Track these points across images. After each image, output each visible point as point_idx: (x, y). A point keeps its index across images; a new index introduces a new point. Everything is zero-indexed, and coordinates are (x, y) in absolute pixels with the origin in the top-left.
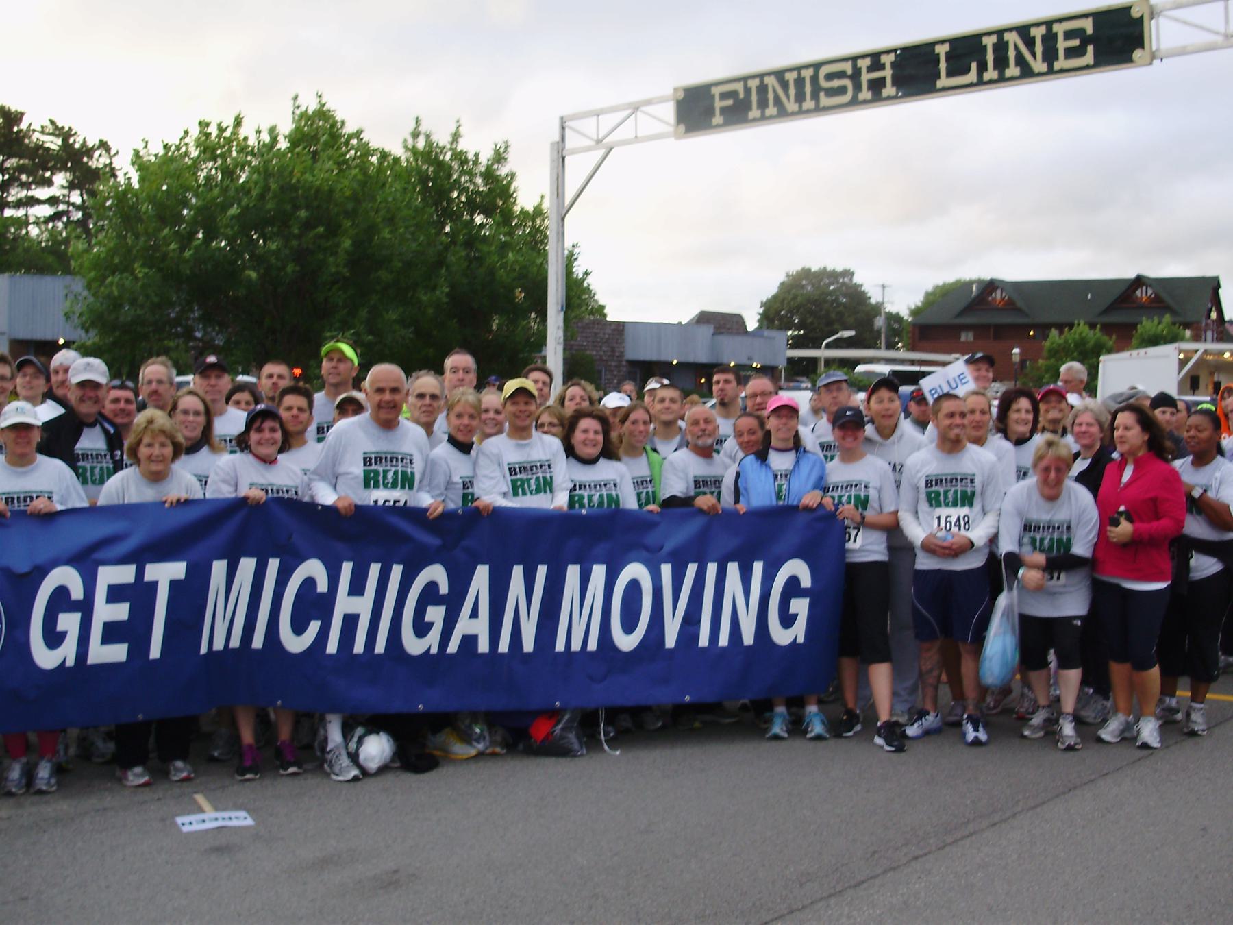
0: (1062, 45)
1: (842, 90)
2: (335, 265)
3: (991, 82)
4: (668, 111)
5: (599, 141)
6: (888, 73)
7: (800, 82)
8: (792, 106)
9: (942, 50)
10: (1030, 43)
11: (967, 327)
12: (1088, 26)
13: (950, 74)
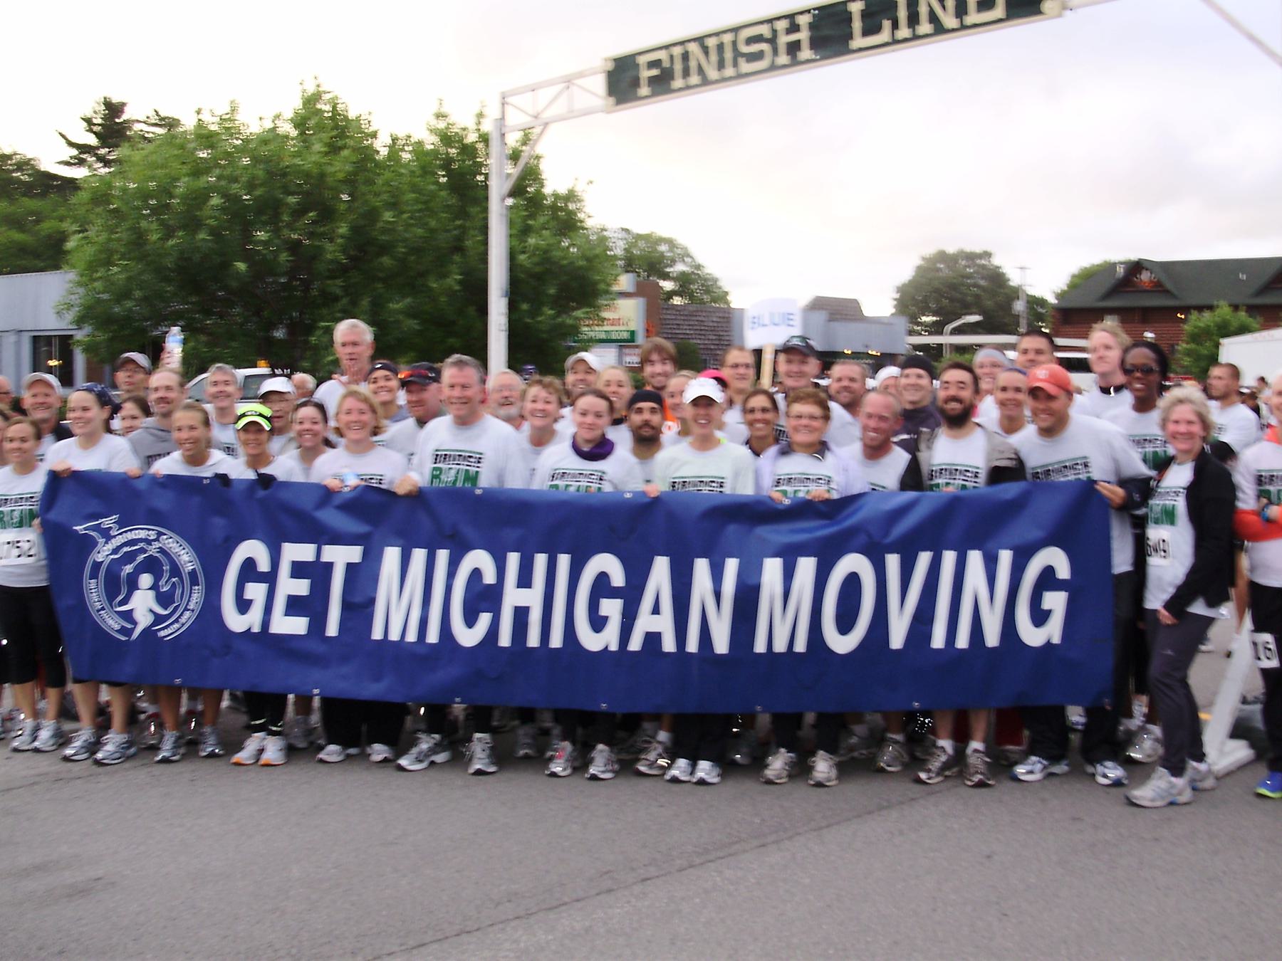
1: (758, 56)
2: (332, 251)
4: (599, 84)
6: (803, 35)
7: (720, 47)
8: (713, 74)
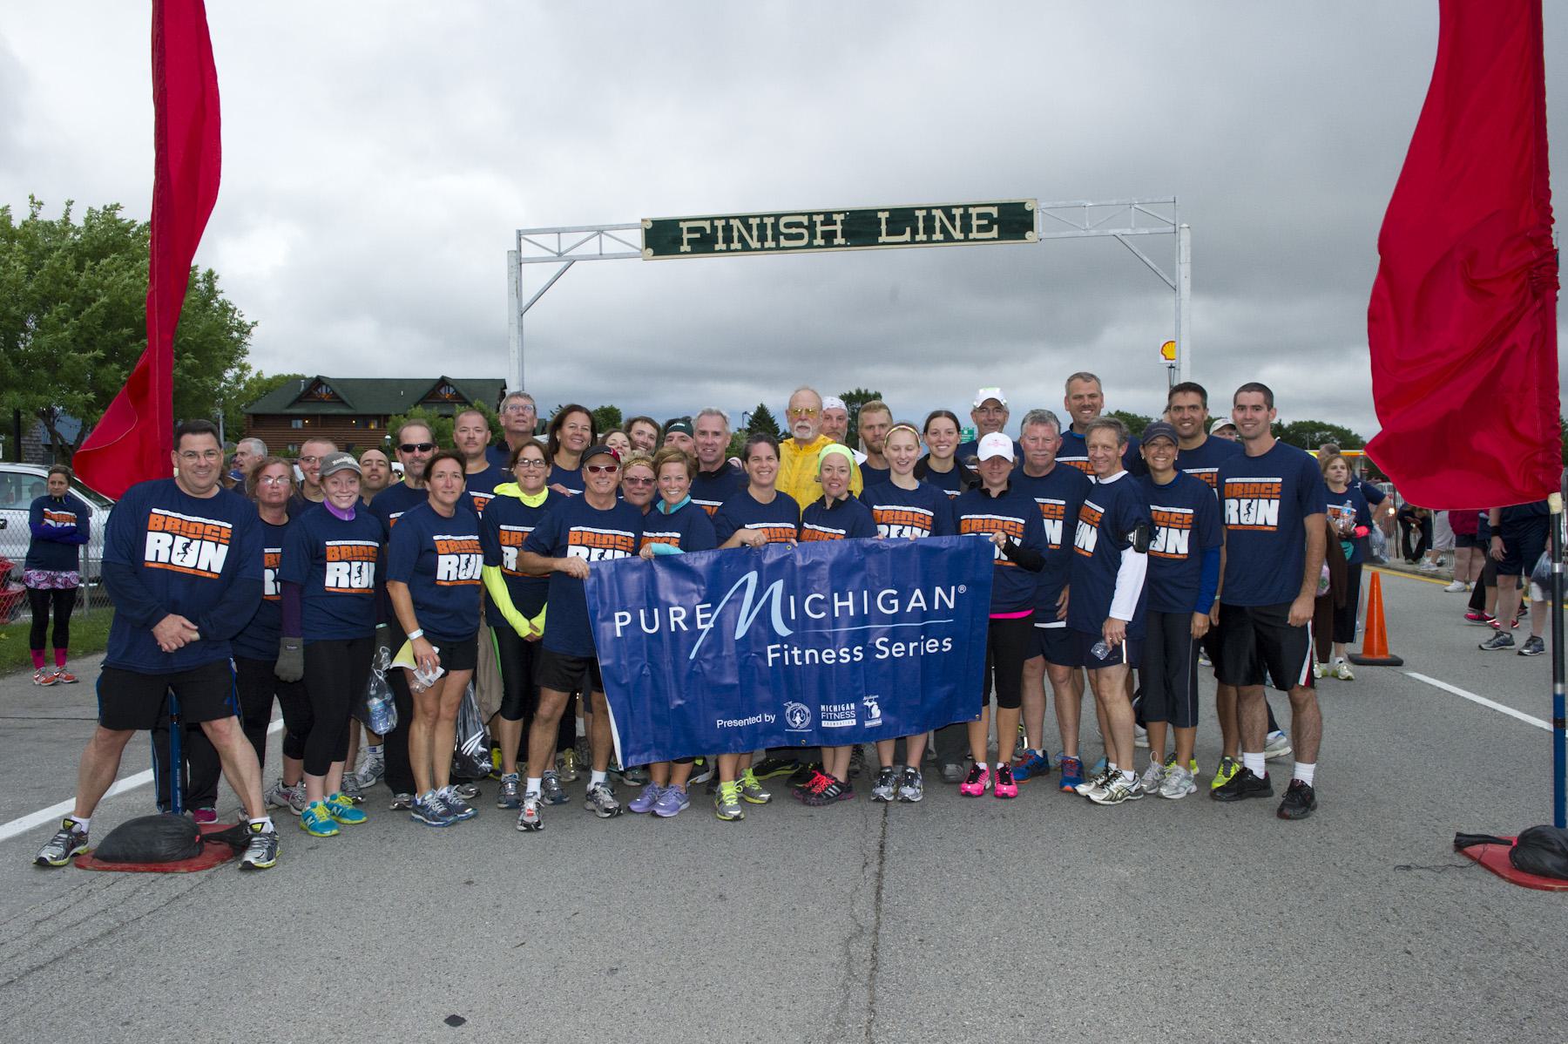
0: (975, 223)
1: (800, 236)
3: (921, 242)
4: (637, 238)
5: (560, 254)
6: (838, 228)
9: (883, 216)
10: (952, 218)
11: (301, 417)
12: (994, 212)
13: (888, 234)
